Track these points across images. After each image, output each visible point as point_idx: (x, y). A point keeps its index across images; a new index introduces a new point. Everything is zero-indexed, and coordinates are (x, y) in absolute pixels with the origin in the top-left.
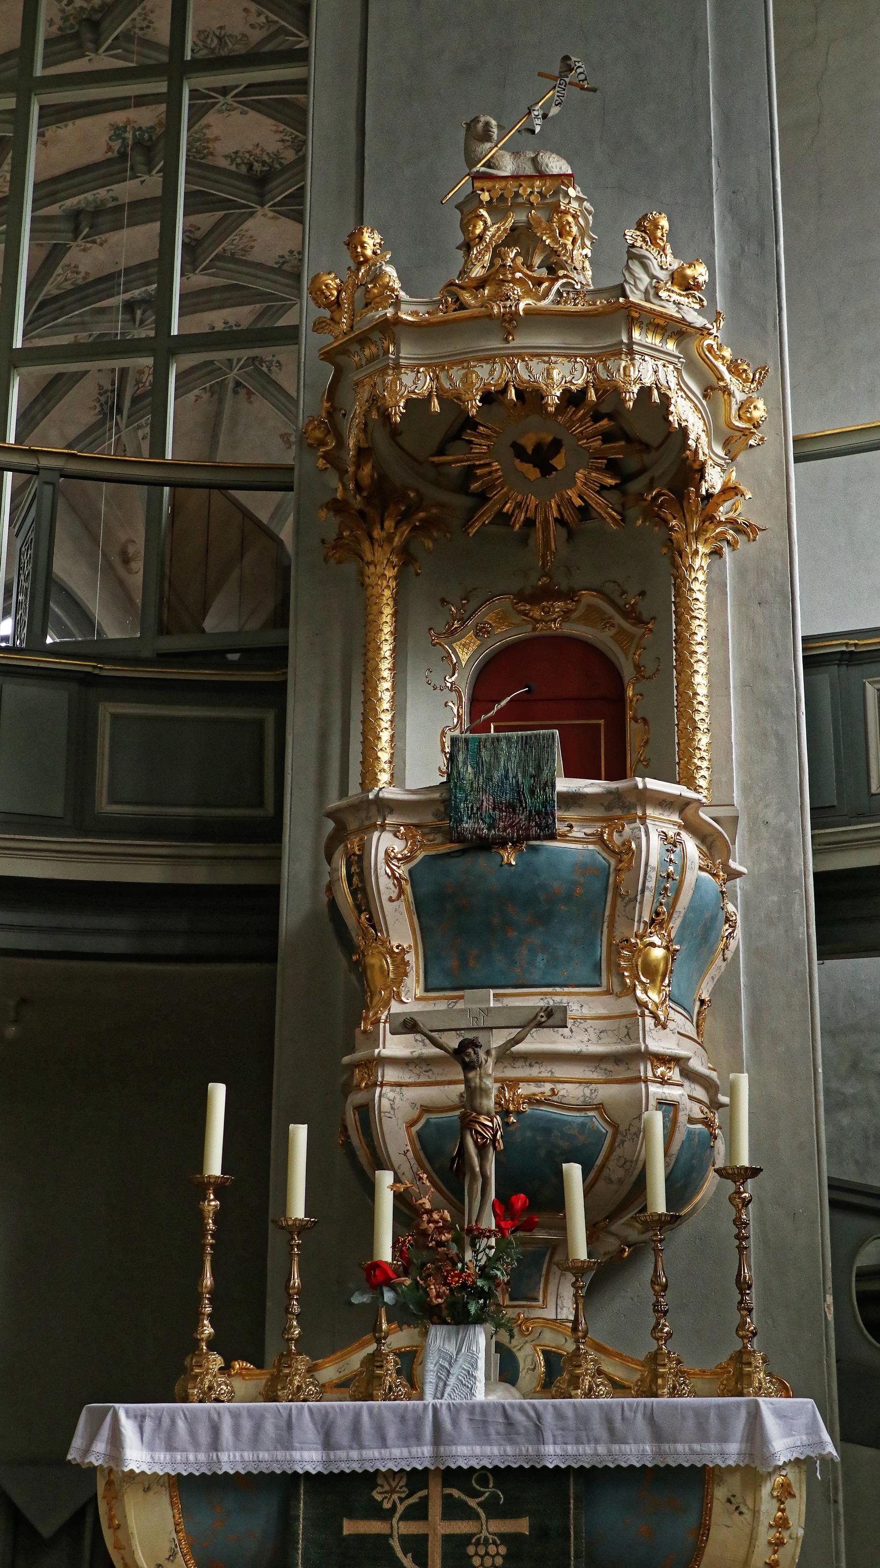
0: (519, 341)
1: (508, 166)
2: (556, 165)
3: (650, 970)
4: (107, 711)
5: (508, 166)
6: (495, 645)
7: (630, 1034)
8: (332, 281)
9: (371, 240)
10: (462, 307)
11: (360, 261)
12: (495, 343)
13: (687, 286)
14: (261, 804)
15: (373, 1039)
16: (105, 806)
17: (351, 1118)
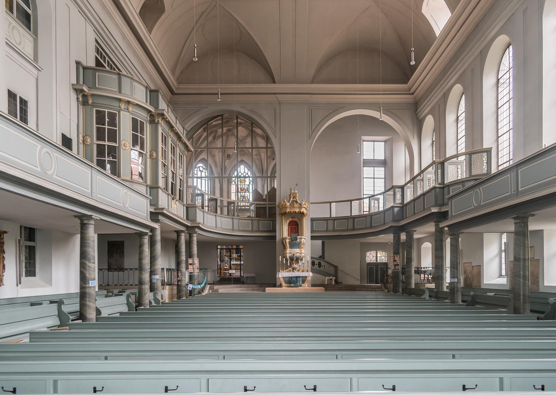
0: (295, 208)
1: (293, 192)
2: (296, 192)
3: (302, 248)
4: (260, 222)
5: (293, 192)
6: (290, 221)
7: (301, 252)
8: (283, 203)
9: (286, 200)
10: (291, 206)
11: (285, 202)
12: (293, 208)
13: (305, 205)
14: (271, 228)
15: (286, 251)
16: (261, 229)
17: (285, 256)
